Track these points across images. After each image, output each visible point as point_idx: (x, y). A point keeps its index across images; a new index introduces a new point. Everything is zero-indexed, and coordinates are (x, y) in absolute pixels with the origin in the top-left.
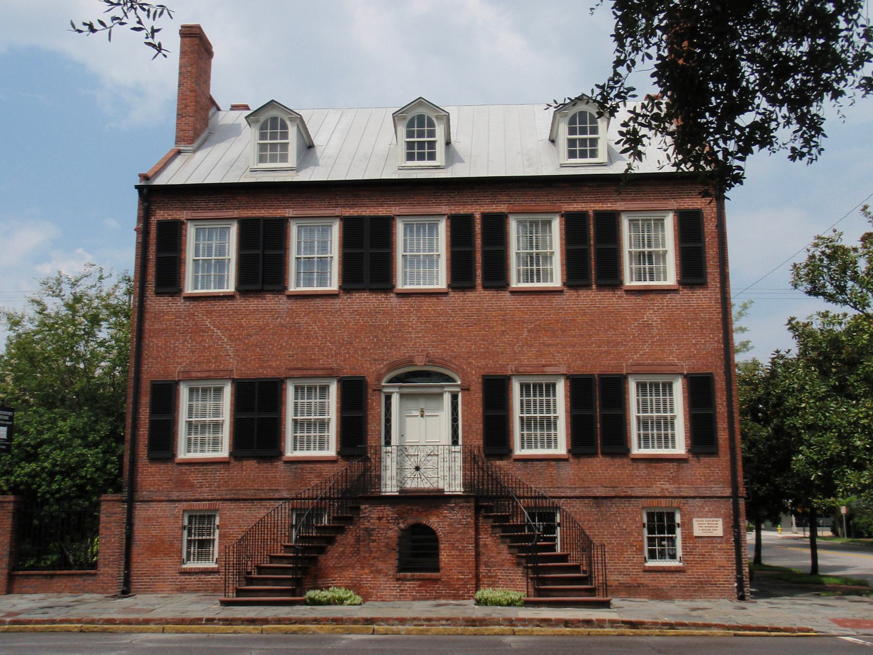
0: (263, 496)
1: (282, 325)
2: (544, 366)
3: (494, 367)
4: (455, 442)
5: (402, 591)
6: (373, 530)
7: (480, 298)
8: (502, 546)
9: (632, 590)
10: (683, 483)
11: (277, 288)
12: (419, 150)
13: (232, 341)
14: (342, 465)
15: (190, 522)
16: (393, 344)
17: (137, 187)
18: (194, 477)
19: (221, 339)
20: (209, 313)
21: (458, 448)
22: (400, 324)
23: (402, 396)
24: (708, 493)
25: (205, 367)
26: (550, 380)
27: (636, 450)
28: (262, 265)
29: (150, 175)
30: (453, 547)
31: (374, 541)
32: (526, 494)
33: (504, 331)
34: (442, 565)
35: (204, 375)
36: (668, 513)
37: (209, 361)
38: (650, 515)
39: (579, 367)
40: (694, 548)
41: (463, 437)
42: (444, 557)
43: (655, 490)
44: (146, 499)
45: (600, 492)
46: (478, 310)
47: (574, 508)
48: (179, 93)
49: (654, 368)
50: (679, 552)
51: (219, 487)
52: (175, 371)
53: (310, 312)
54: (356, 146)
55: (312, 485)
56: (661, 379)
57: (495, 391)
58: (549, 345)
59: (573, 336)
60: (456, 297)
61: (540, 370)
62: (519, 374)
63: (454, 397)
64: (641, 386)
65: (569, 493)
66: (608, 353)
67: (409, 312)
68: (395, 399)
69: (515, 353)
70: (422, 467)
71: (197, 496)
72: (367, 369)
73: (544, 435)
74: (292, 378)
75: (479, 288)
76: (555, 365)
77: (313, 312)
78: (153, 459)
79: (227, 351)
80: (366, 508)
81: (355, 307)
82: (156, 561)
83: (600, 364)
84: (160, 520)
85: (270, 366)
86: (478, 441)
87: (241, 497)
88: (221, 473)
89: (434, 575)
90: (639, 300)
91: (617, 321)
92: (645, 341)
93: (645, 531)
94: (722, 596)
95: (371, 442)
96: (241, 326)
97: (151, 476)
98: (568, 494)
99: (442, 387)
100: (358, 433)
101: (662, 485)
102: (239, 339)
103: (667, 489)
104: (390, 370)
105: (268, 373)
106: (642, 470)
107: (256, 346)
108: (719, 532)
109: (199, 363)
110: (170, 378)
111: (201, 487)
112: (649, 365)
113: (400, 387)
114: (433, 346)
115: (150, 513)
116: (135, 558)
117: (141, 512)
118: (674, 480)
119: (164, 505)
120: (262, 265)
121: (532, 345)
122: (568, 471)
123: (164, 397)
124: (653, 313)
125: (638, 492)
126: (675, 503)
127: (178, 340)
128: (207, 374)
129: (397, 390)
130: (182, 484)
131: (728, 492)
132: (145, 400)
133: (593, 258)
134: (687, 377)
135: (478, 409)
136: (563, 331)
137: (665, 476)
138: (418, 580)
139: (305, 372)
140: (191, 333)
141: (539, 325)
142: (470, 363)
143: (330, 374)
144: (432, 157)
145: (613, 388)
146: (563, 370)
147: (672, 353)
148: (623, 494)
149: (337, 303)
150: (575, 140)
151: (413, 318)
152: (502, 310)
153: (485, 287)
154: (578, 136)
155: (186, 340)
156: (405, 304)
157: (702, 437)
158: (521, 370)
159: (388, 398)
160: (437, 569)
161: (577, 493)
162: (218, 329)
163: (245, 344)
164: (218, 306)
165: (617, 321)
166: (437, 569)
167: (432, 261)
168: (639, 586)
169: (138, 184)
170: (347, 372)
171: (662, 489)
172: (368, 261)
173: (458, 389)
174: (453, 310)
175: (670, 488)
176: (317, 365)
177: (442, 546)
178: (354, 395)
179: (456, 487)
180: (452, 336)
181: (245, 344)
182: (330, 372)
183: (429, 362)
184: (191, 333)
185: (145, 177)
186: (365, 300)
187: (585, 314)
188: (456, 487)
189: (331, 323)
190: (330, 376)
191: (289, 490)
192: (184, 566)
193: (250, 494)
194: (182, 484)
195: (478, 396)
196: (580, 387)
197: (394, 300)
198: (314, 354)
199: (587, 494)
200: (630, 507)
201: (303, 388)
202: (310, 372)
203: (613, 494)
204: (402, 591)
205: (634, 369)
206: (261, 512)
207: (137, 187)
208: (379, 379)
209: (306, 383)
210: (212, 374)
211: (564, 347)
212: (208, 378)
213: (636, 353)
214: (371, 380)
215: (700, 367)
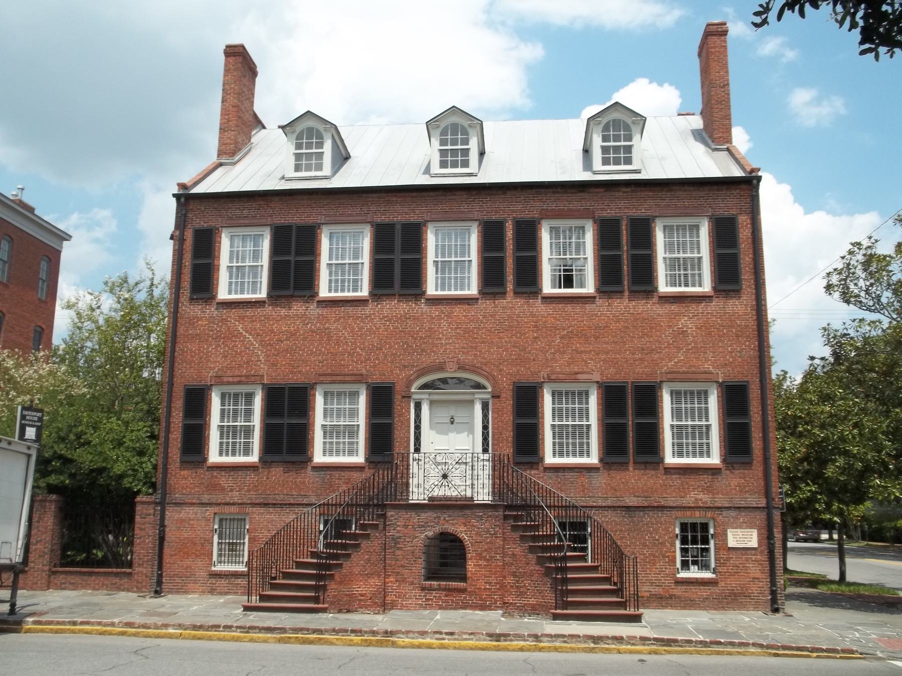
0: (292, 501)
1: (313, 331)
2: (576, 373)
3: (526, 376)
4: (485, 451)
5: (427, 600)
6: (400, 537)
7: (511, 303)
8: (530, 556)
9: (663, 601)
10: (718, 493)
11: (308, 293)
12: (453, 156)
15: (221, 526)
16: (423, 350)
17: (174, 195)
18: (225, 480)
19: (252, 344)
20: (241, 318)
21: (486, 456)
23: (432, 403)
24: (743, 504)
25: (237, 373)
27: (670, 459)
28: (293, 272)
29: (189, 184)
30: (480, 557)
31: (399, 549)
32: (556, 504)
33: (536, 338)
34: (469, 574)
35: (236, 380)
37: (240, 366)
38: (684, 527)
39: (613, 375)
40: (728, 559)
41: (493, 444)
42: (471, 566)
43: (690, 499)
46: (509, 317)
48: (222, 109)
49: (689, 376)
50: (713, 565)
51: (249, 491)
52: (208, 376)
53: (340, 318)
54: (390, 155)
55: (341, 491)
57: (526, 401)
58: (582, 352)
59: (607, 343)
60: (486, 305)
61: (573, 377)
62: (550, 380)
63: (485, 407)
64: (676, 395)
65: (600, 503)
66: (641, 360)
67: (439, 318)
70: (450, 475)
71: (228, 500)
72: (394, 375)
74: (322, 383)
75: (510, 294)
76: (588, 373)
77: (344, 317)
78: (184, 464)
79: (258, 356)
80: (392, 516)
82: (188, 562)
83: (633, 372)
85: (300, 372)
86: (508, 450)
87: (270, 501)
88: (251, 477)
91: (651, 328)
92: (679, 349)
94: (756, 608)
95: (398, 448)
96: (272, 331)
97: (182, 480)
98: (600, 504)
99: (473, 394)
101: (696, 496)
102: (270, 345)
103: (701, 500)
104: (418, 377)
105: (296, 379)
106: (676, 480)
108: (754, 543)
111: (232, 490)
112: (684, 373)
113: (430, 394)
114: (464, 353)
115: (183, 515)
116: (167, 559)
118: (708, 490)
119: (196, 509)
120: (293, 272)
121: (564, 352)
122: (600, 480)
123: (196, 402)
126: (709, 514)
127: (211, 345)
128: (238, 379)
129: (427, 396)
130: (213, 487)
131: (763, 503)
133: (626, 266)
134: (720, 385)
135: (508, 417)
136: (596, 338)
137: (699, 487)
138: (445, 590)
139: (334, 378)
140: (224, 338)
141: (572, 332)
142: (501, 370)
143: (359, 379)
144: (465, 164)
145: (647, 398)
146: (597, 377)
147: (707, 360)
148: (656, 504)
149: (368, 310)
150: (609, 147)
151: (444, 323)
152: (533, 315)
153: (517, 293)
154: (612, 144)
155: (219, 346)
156: (435, 311)
158: (553, 377)
159: (418, 406)
160: (464, 579)
161: (609, 503)
162: (250, 334)
163: (276, 350)
165: (651, 328)
166: (464, 579)
167: (462, 265)
168: (671, 597)
169: (176, 192)
171: (696, 499)
172: (396, 268)
173: (488, 396)
174: (484, 317)
177: (469, 556)
178: (383, 401)
179: (484, 496)
181: (276, 350)
182: (358, 378)
183: (459, 368)
184: (224, 338)
185: (182, 186)
186: (393, 307)
187: (618, 321)
188: (484, 496)
189: (361, 329)
190: (360, 382)
193: (279, 499)
194: (213, 487)
195: (508, 403)
196: (613, 397)
197: (423, 307)
198: (344, 360)
199: (619, 504)
200: (663, 517)
201: (332, 394)
202: (339, 378)
203: (646, 504)
204: (427, 600)
205: (669, 376)
206: (289, 517)
207: (174, 195)
208: (409, 386)
209: (335, 388)
210: (243, 378)
211: (598, 354)
212: (239, 383)
215: (735, 376)
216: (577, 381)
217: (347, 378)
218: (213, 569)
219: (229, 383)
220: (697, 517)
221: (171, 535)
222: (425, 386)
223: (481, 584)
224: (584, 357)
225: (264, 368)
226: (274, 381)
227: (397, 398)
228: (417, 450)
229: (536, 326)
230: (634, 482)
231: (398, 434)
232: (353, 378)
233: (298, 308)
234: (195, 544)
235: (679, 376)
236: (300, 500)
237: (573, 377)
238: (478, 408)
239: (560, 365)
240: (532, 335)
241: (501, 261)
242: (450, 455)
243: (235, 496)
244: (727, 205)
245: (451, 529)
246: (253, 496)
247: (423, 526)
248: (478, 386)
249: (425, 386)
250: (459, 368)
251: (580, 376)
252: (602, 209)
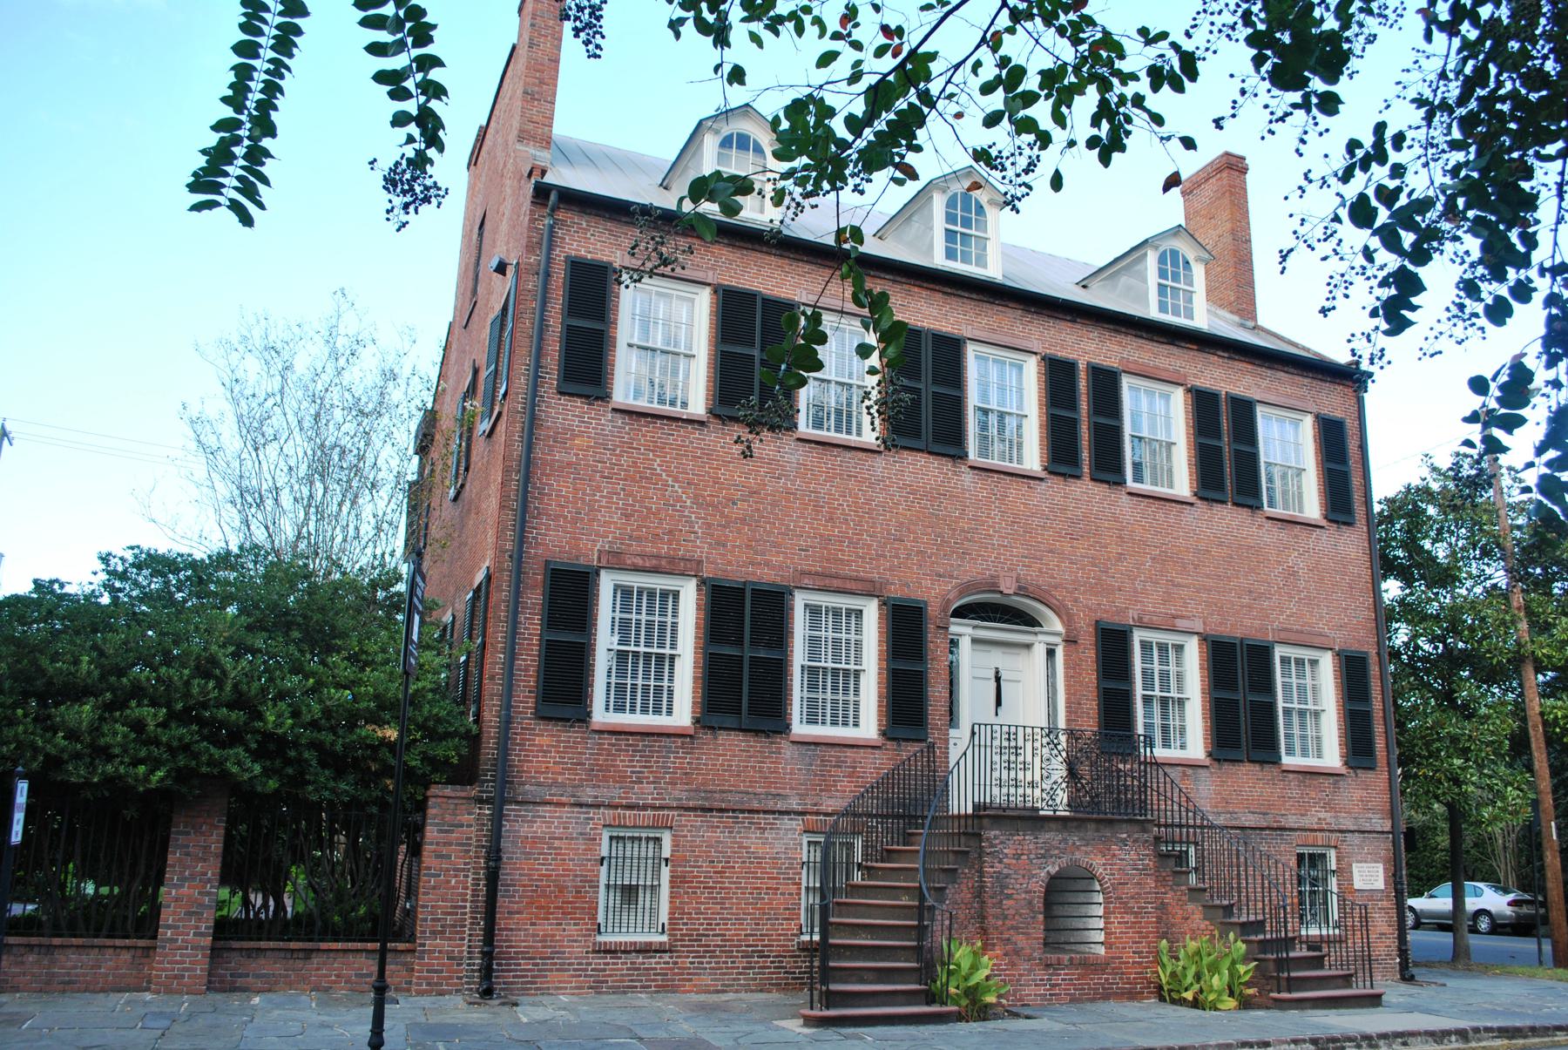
0: (756, 805)
6: (1007, 876)
8: (1190, 907)
13: (700, 506)
19: (679, 499)
20: (656, 448)
22: (976, 519)
31: (1009, 897)
32: (1191, 822)
38: (1300, 857)
44: (530, 798)
45: (1249, 820)
50: (1335, 914)
52: (590, 551)
58: (1179, 585)
59: (1208, 576)
60: (1056, 489)
63: (1051, 653)
66: (1250, 607)
68: (965, 644)
69: (1135, 591)
75: (1087, 478)
76: (1188, 618)
80: (996, 837)
81: (908, 479)
82: (546, 927)
83: (1242, 626)
84: (557, 843)
85: (767, 564)
87: (716, 804)
97: (543, 751)
100: (911, 702)
102: (712, 504)
105: (766, 575)
107: (743, 521)
108: (1380, 884)
109: (639, 539)
110: (582, 561)
112: (1297, 631)
113: (975, 627)
115: (538, 828)
117: (524, 827)
118: (1328, 806)
123: (570, 594)
125: (1291, 821)
129: (969, 630)
130: (599, 774)
131: (1387, 826)
132: (535, 598)
135: (1090, 677)
162: (676, 480)
163: (722, 515)
164: (677, 435)
170: (896, 592)
173: (1057, 640)
176: (846, 571)
178: (907, 629)
180: (1051, 551)
181: (722, 515)
182: (868, 586)
187: (1221, 544)
190: (870, 595)
191: (802, 796)
192: (600, 939)
195: (1089, 654)
197: (968, 477)
199: (1234, 823)
202: (836, 583)
205: (1283, 635)
212: (655, 571)
214: (933, 610)
217: (849, 585)
218: (600, 939)
219: (637, 569)
221: (516, 868)
224: (1184, 592)
225: (701, 548)
226: (720, 575)
232: (819, 583)
234: (562, 889)
236: (770, 805)
240: (1115, 549)
241: (1073, 424)
243: (647, 792)
244: (1333, 401)
246: (679, 793)
247: (1043, 856)
252: (1196, 376)
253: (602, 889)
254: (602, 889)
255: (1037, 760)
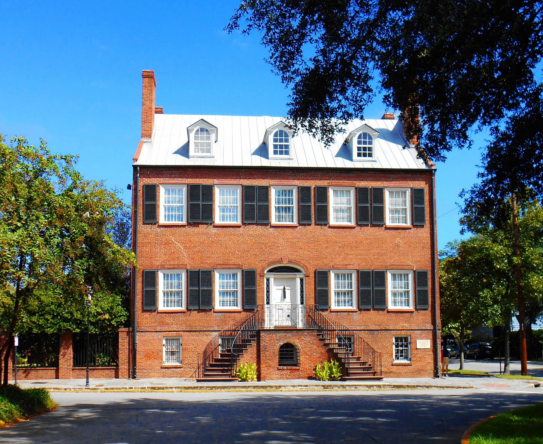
0: (205, 329)
1: (212, 242)
2: (346, 265)
3: (321, 266)
7: (313, 229)
9: (390, 374)
14: (244, 314)
16: (271, 252)
18: (168, 319)
19: (180, 248)
20: (173, 234)
25: (172, 263)
26: (349, 272)
28: (200, 209)
36: (405, 338)
42: (302, 359)
47: (363, 334)
49: (400, 267)
51: (181, 324)
56: (403, 272)
57: (322, 278)
61: (345, 267)
62: (333, 268)
63: (302, 280)
64: (394, 276)
65: (358, 328)
68: (272, 280)
69: (332, 258)
70: (287, 315)
73: (341, 298)
85: (206, 263)
86: (312, 302)
87: (193, 330)
88: (181, 317)
89: (297, 368)
90: (394, 232)
92: (395, 253)
93: (394, 346)
94: (429, 376)
95: (259, 302)
96: (190, 241)
101: (402, 324)
104: (269, 265)
105: (205, 267)
107: (199, 252)
120: (200, 209)
121: (341, 254)
122: (356, 316)
124: (399, 238)
128: (173, 266)
130: (163, 323)
133: (369, 211)
141: (344, 244)
145: (380, 277)
147: (408, 259)
153: (316, 224)
157: (421, 300)
159: (268, 280)
161: (362, 328)
162: (179, 243)
164: (177, 230)
165: (382, 243)
168: (391, 372)
175: (406, 325)
176: (231, 262)
178: (250, 278)
180: (300, 249)
187: (366, 239)
188: (300, 326)
190: (238, 268)
191: (218, 326)
193: (198, 328)
194: (163, 323)
199: (367, 329)
202: (227, 266)
203: (379, 329)
208: (263, 271)
210: (176, 266)
212: (174, 268)
213: (391, 259)
214: (258, 271)
216: (346, 269)
217: (232, 266)
219: (168, 269)
220: (403, 334)
222: (270, 271)
223: (307, 367)
224: (350, 257)
225: (186, 261)
227: (258, 277)
228: (268, 303)
229: (327, 241)
230: (373, 318)
231: (258, 295)
233: (202, 228)
235: (395, 267)
237: (345, 267)
238: (298, 281)
239: (338, 261)
240: (324, 245)
242: (282, 306)
243: (175, 328)
245: (291, 341)
248: (298, 271)
249: (270, 271)
250: (289, 262)
251: (348, 266)
253: (164, 353)
254: (164, 353)
255: (277, 314)
